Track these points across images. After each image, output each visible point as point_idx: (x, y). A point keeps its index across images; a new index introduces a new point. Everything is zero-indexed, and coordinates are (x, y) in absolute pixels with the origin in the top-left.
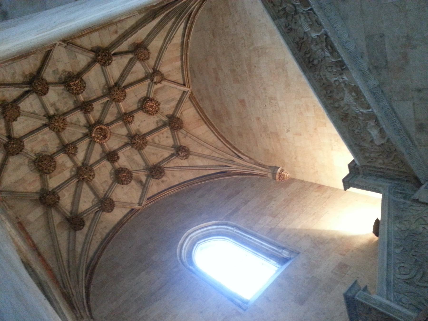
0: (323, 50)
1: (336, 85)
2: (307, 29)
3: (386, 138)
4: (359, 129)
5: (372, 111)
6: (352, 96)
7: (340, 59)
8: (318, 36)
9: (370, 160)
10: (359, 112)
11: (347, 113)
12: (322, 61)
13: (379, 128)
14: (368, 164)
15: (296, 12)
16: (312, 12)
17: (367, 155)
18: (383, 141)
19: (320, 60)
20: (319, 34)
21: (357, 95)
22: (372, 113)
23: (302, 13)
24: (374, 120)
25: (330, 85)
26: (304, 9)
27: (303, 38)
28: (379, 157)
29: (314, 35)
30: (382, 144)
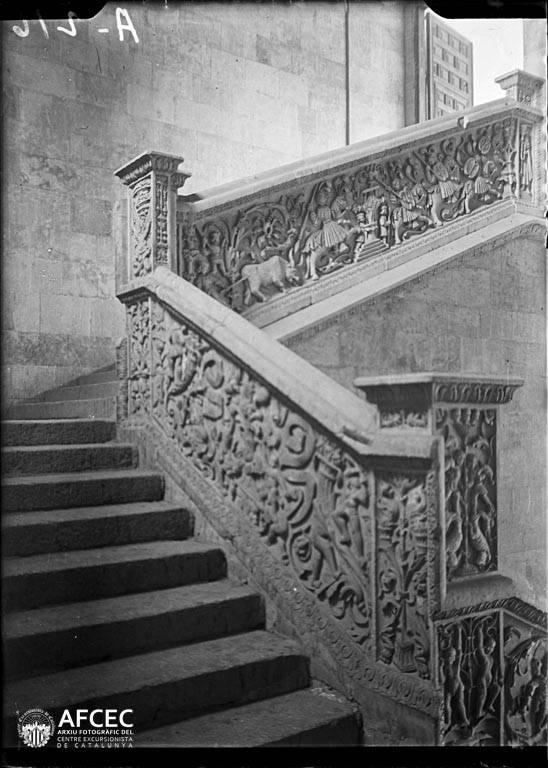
0: (414, 209)
1: (358, 213)
2: (446, 189)
3: (261, 294)
4: (276, 235)
5: (310, 277)
6: (339, 244)
7: (398, 240)
8: (431, 206)
9: (206, 241)
10: (312, 247)
11: (307, 217)
12: (397, 197)
13: (282, 284)
14: (193, 230)
15: (464, 177)
16: (462, 210)
17: (217, 237)
18: (254, 287)
19: (400, 195)
20: (433, 209)
21: (340, 254)
22: (306, 276)
23: (462, 189)
24: (297, 278)
25: (360, 197)
26: (468, 196)
27: (431, 173)
28: (215, 268)
29: (434, 200)
30: (246, 284)
